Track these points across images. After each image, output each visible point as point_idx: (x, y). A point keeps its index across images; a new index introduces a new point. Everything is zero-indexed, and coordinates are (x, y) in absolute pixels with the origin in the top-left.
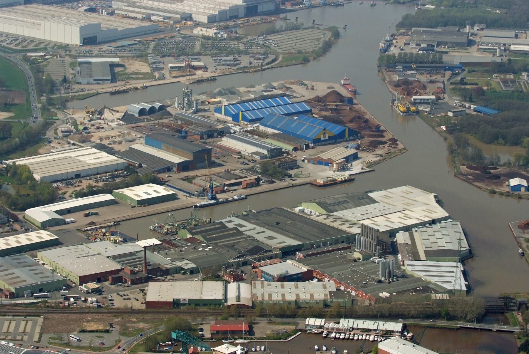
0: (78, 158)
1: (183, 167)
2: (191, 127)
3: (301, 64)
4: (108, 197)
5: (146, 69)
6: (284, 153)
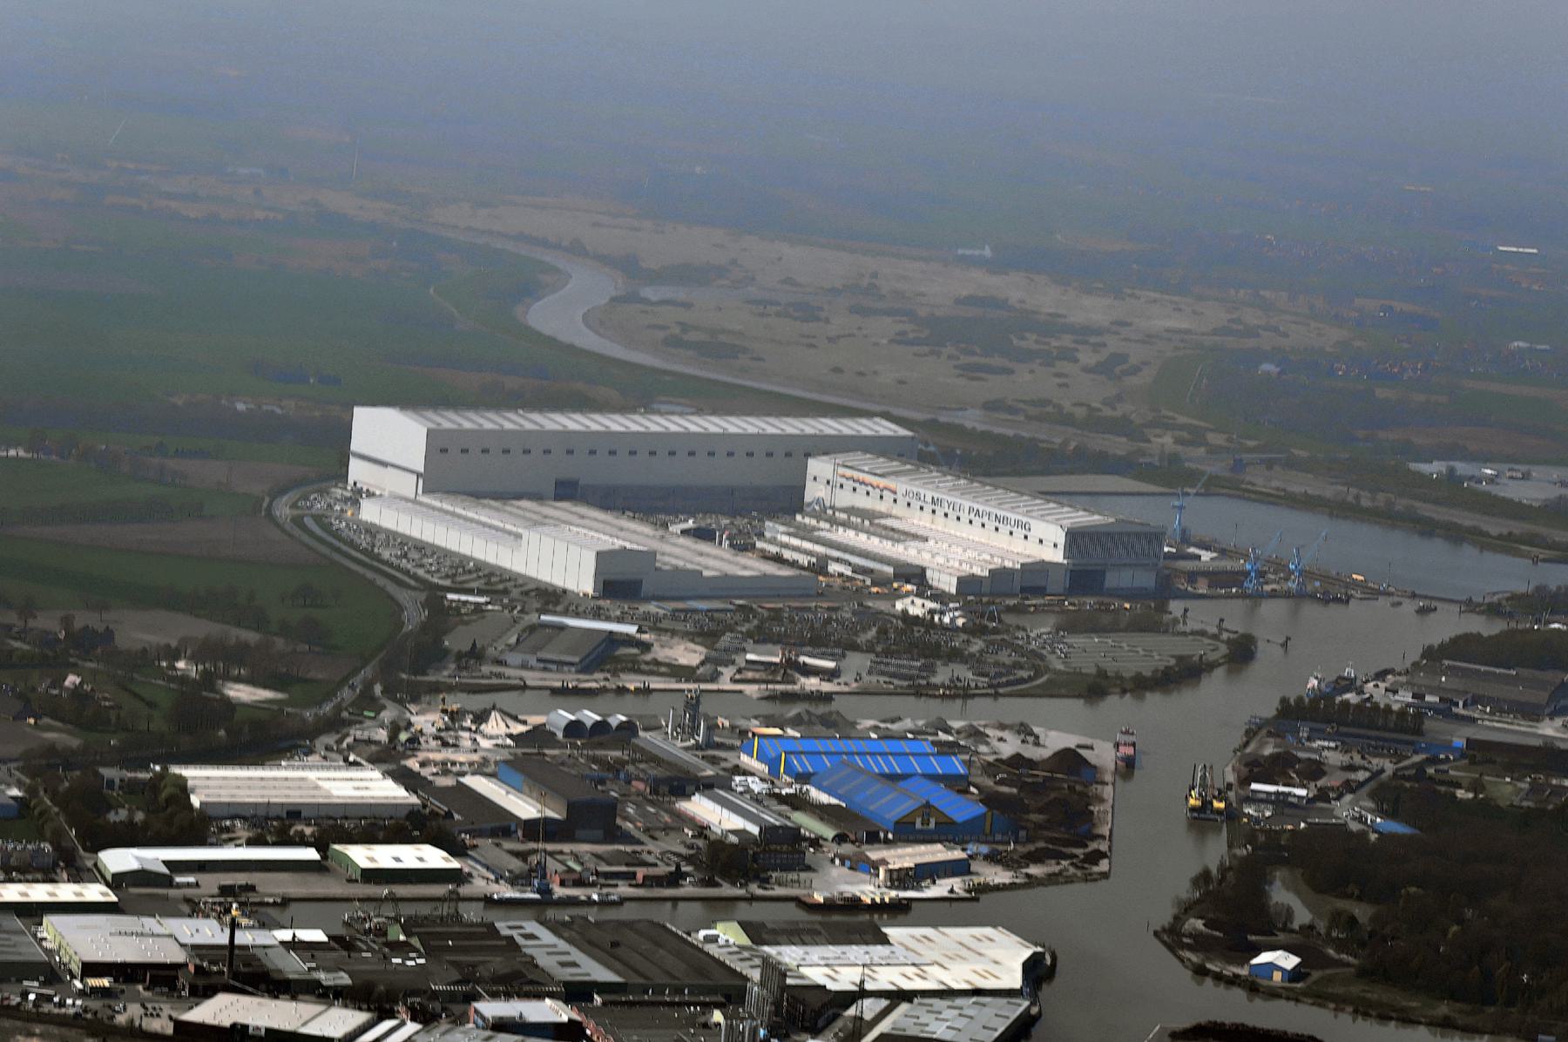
0: (320, 783)
1: (533, 829)
2: (642, 766)
3: (1079, 696)
4: (311, 854)
5: (688, 654)
6: (805, 839)
